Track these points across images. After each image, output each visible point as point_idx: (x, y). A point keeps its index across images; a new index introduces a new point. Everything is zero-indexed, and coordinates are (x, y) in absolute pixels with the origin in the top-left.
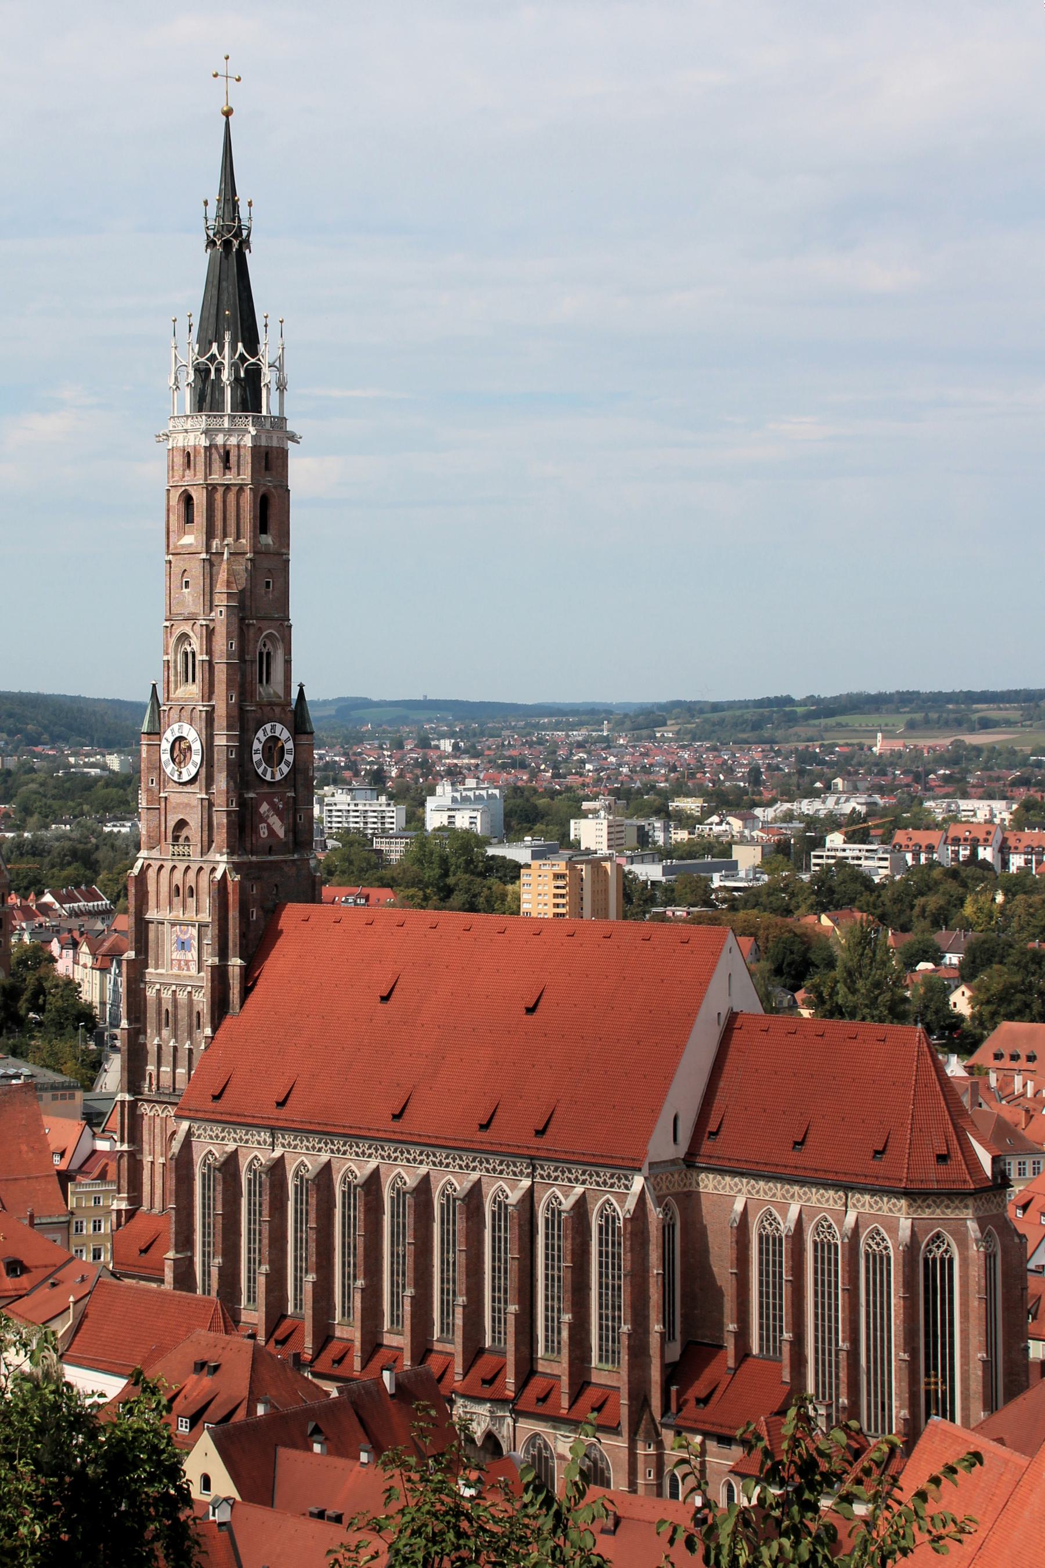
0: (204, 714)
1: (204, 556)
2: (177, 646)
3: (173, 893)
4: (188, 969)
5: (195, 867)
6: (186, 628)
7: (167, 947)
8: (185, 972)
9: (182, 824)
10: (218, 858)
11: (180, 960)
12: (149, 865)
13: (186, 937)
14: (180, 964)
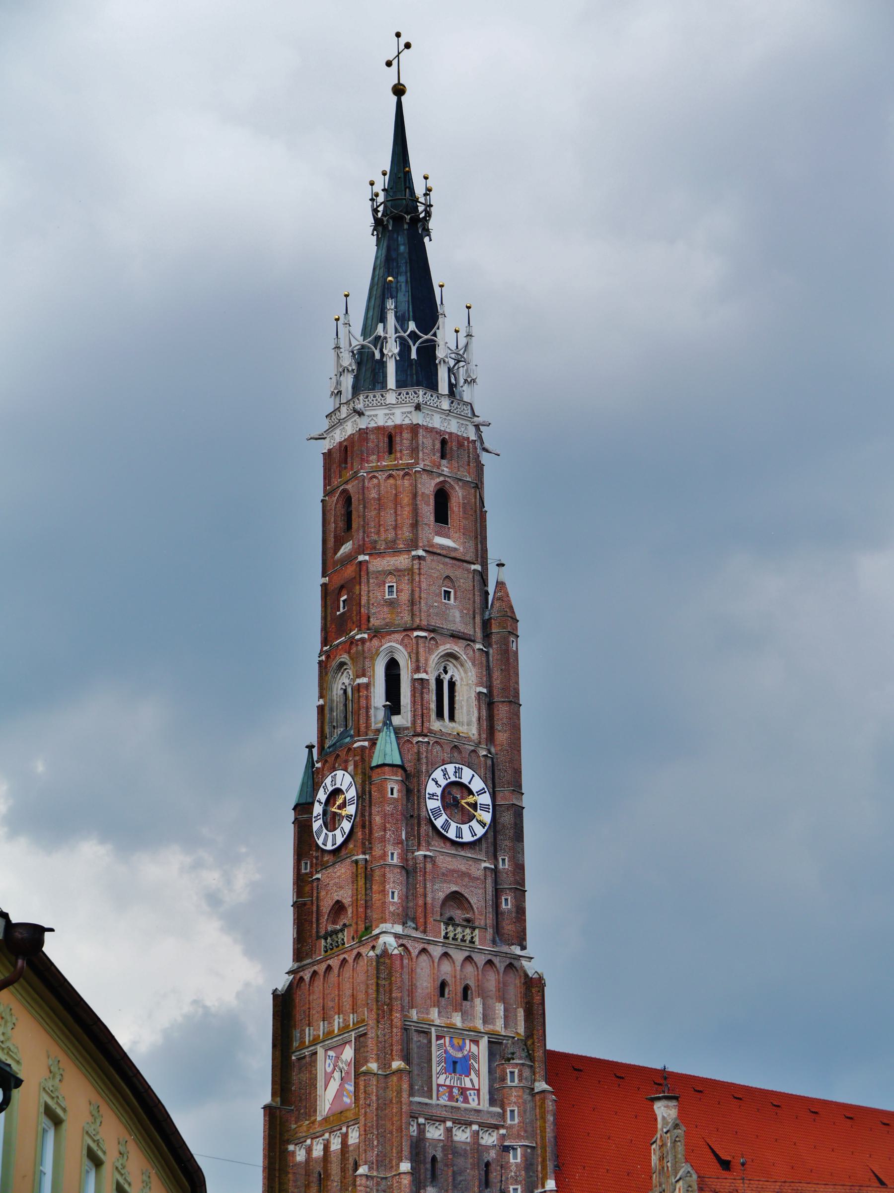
3: (438, 992)
4: (466, 1100)
5: (480, 959)
6: (456, 648)
7: (435, 1069)
8: (460, 1104)
9: (456, 898)
11: (451, 1088)
13: (460, 1055)
14: (451, 1093)
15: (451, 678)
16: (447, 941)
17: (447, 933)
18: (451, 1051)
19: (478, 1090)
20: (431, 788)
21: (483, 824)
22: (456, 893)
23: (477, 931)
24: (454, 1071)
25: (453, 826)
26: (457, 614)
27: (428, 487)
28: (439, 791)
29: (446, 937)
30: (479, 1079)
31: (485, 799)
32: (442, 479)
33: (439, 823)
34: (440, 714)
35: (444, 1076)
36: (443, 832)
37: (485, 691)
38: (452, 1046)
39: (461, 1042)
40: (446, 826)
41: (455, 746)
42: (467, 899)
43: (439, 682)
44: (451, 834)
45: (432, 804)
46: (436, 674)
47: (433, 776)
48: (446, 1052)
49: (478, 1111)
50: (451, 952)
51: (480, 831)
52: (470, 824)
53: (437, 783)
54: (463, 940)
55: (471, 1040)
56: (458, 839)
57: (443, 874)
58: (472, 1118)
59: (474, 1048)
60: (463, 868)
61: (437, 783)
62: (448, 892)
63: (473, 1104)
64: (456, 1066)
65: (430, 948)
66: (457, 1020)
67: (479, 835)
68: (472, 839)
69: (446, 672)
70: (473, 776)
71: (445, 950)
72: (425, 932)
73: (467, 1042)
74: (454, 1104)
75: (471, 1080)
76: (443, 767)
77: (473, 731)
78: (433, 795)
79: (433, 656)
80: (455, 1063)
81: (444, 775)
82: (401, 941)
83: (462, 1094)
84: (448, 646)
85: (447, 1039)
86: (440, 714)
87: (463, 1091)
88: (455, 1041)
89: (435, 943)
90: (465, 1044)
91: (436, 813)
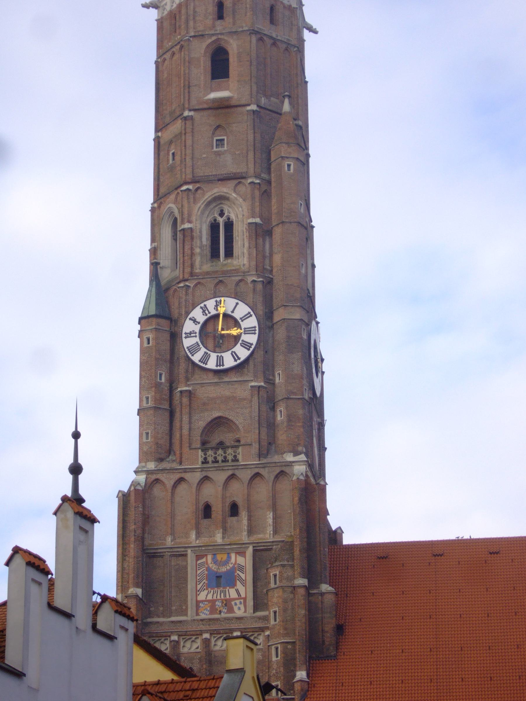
0: (260, 287)
1: (254, 107)
2: (203, 213)
3: (201, 514)
4: (231, 610)
5: (245, 475)
8: (223, 615)
9: (219, 423)
10: (289, 457)
11: (213, 602)
12: (157, 480)
13: (224, 569)
15: (229, 219)
16: (205, 466)
17: (205, 459)
18: (214, 567)
19: (245, 599)
20: (188, 326)
21: (246, 345)
22: (220, 417)
23: (240, 450)
24: (218, 586)
25: (213, 357)
26: (228, 158)
27: (200, 51)
28: (197, 328)
29: (205, 462)
30: (243, 589)
31: (252, 322)
32: (214, 38)
33: (196, 358)
34: (215, 254)
35: (206, 592)
36: (202, 365)
37: (258, 220)
38: (215, 561)
39: (225, 557)
40: (205, 359)
41: (221, 281)
42: (232, 421)
43: (214, 227)
44: (212, 364)
45: (187, 343)
46: (210, 219)
47: (191, 316)
48: (208, 569)
49: (240, 619)
50: (210, 474)
51: (243, 353)
52: (233, 350)
53: (194, 321)
54: (225, 460)
55: (236, 553)
56: (219, 368)
57: (204, 404)
58: (233, 626)
59: (241, 560)
60: (227, 393)
61: (194, 321)
62: (210, 419)
63: (239, 612)
64: (220, 580)
65: (187, 476)
66: (219, 538)
67: (242, 360)
68: (235, 363)
69: (222, 214)
70: (237, 304)
71: (204, 474)
72: (181, 463)
73: (233, 556)
74: (216, 616)
75: (237, 591)
76: (202, 305)
77: (246, 261)
78: (190, 333)
79: (199, 205)
80: (219, 577)
81: (204, 311)
82: (154, 477)
83: (226, 605)
84: (216, 190)
85: (210, 557)
86: (215, 254)
87: (228, 604)
88: (219, 557)
89: (193, 470)
90: (229, 558)
91: (194, 349)
